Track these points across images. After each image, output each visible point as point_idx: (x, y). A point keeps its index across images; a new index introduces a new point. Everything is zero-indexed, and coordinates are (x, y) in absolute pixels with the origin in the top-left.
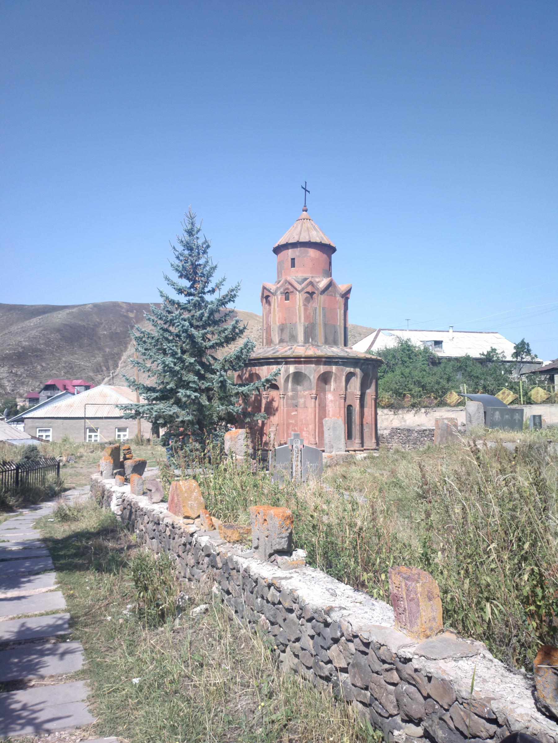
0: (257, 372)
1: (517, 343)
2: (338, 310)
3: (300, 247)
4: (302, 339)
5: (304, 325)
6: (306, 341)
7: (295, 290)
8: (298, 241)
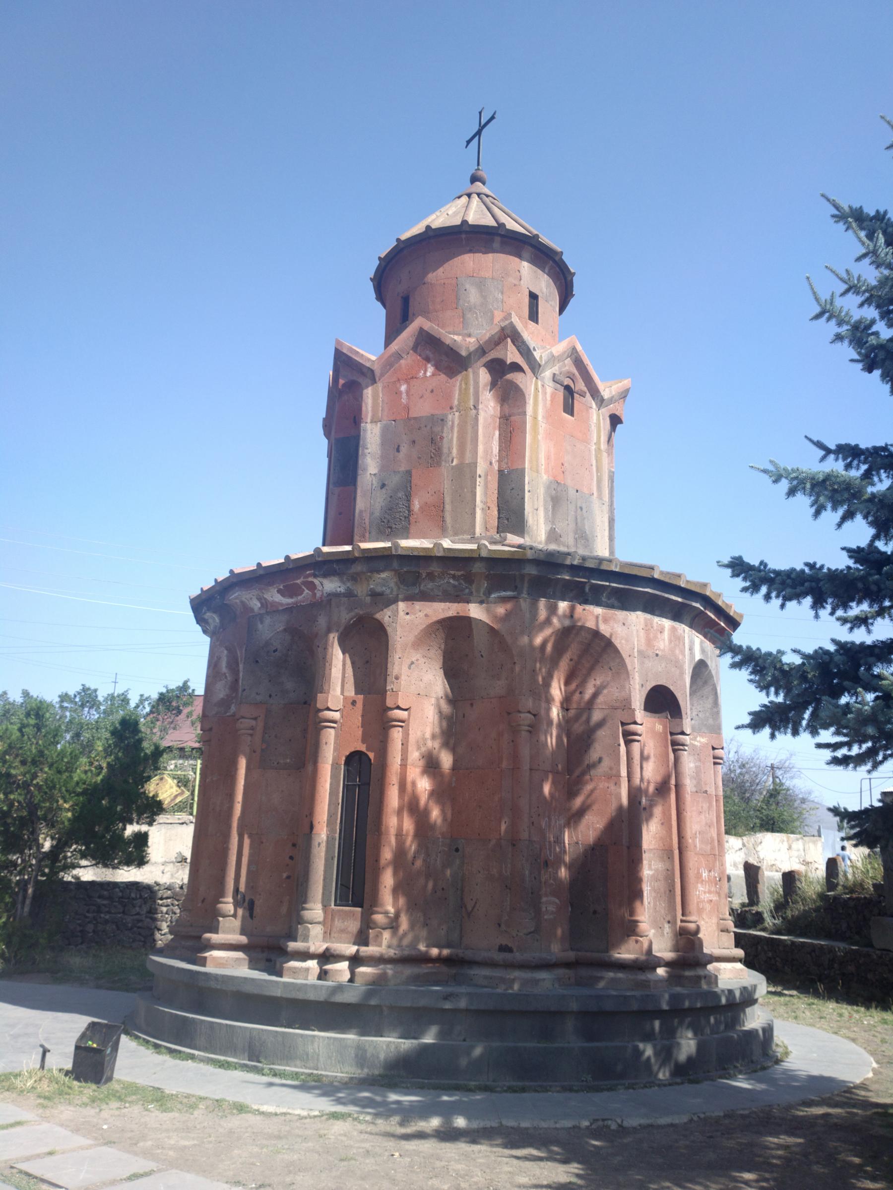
0: (604, 629)
7: (588, 395)
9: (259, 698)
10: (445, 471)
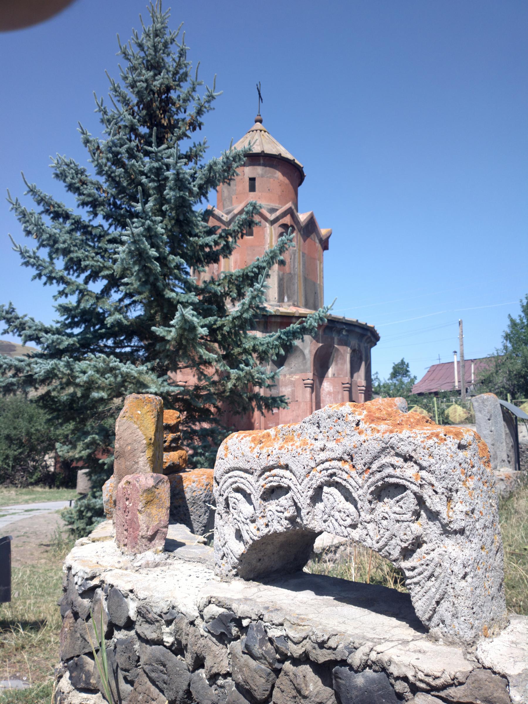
1: (396, 363)
2: (318, 262)
3: (265, 165)
4: (276, 295)
5: (279, 275)
6: (281, 299)
7: (263, 221)
8: (263, 152)
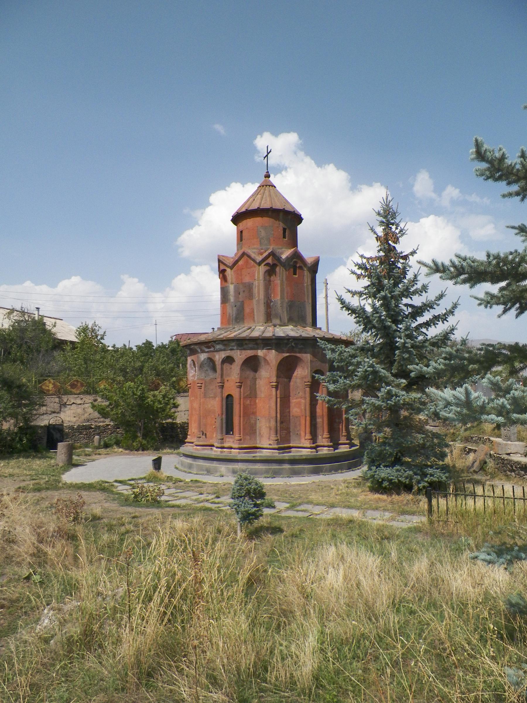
9: (202, 378)
10: (255, 301)
